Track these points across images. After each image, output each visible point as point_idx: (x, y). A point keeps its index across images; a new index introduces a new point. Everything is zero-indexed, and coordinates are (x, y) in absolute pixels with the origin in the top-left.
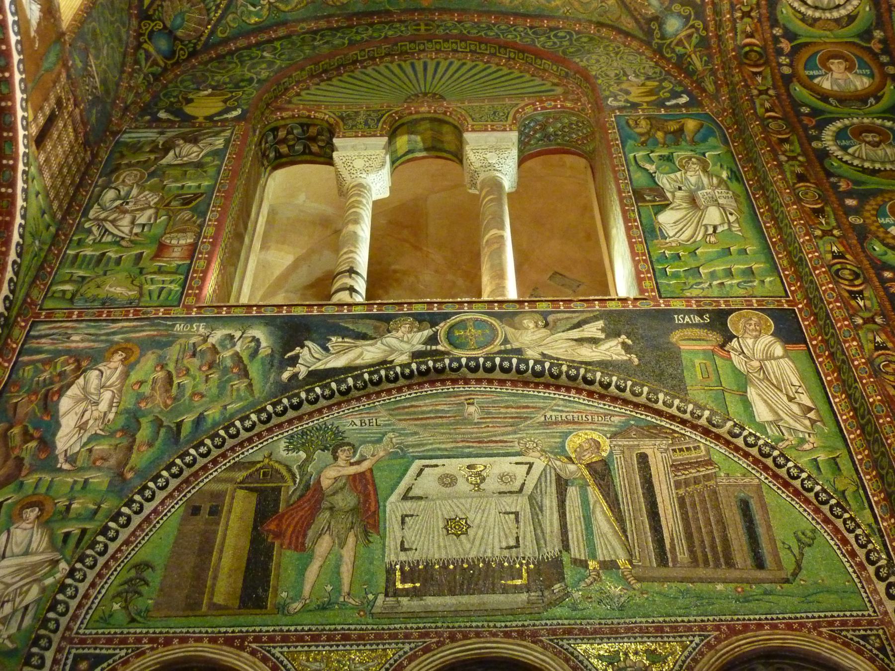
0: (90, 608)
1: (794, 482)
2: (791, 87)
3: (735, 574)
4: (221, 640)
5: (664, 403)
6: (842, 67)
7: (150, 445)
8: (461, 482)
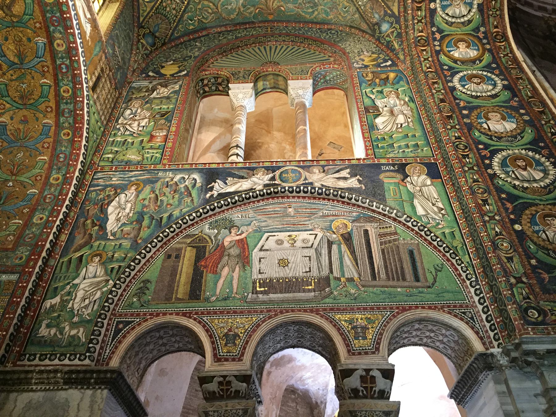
0: (123, 300)
1: (433, 242)
2: (440, 56)
3: (406, 284)
4: (181, 314)
5: (376, 207)
6: (464, 46)
7: (149, 228)
8: (285, 242)
